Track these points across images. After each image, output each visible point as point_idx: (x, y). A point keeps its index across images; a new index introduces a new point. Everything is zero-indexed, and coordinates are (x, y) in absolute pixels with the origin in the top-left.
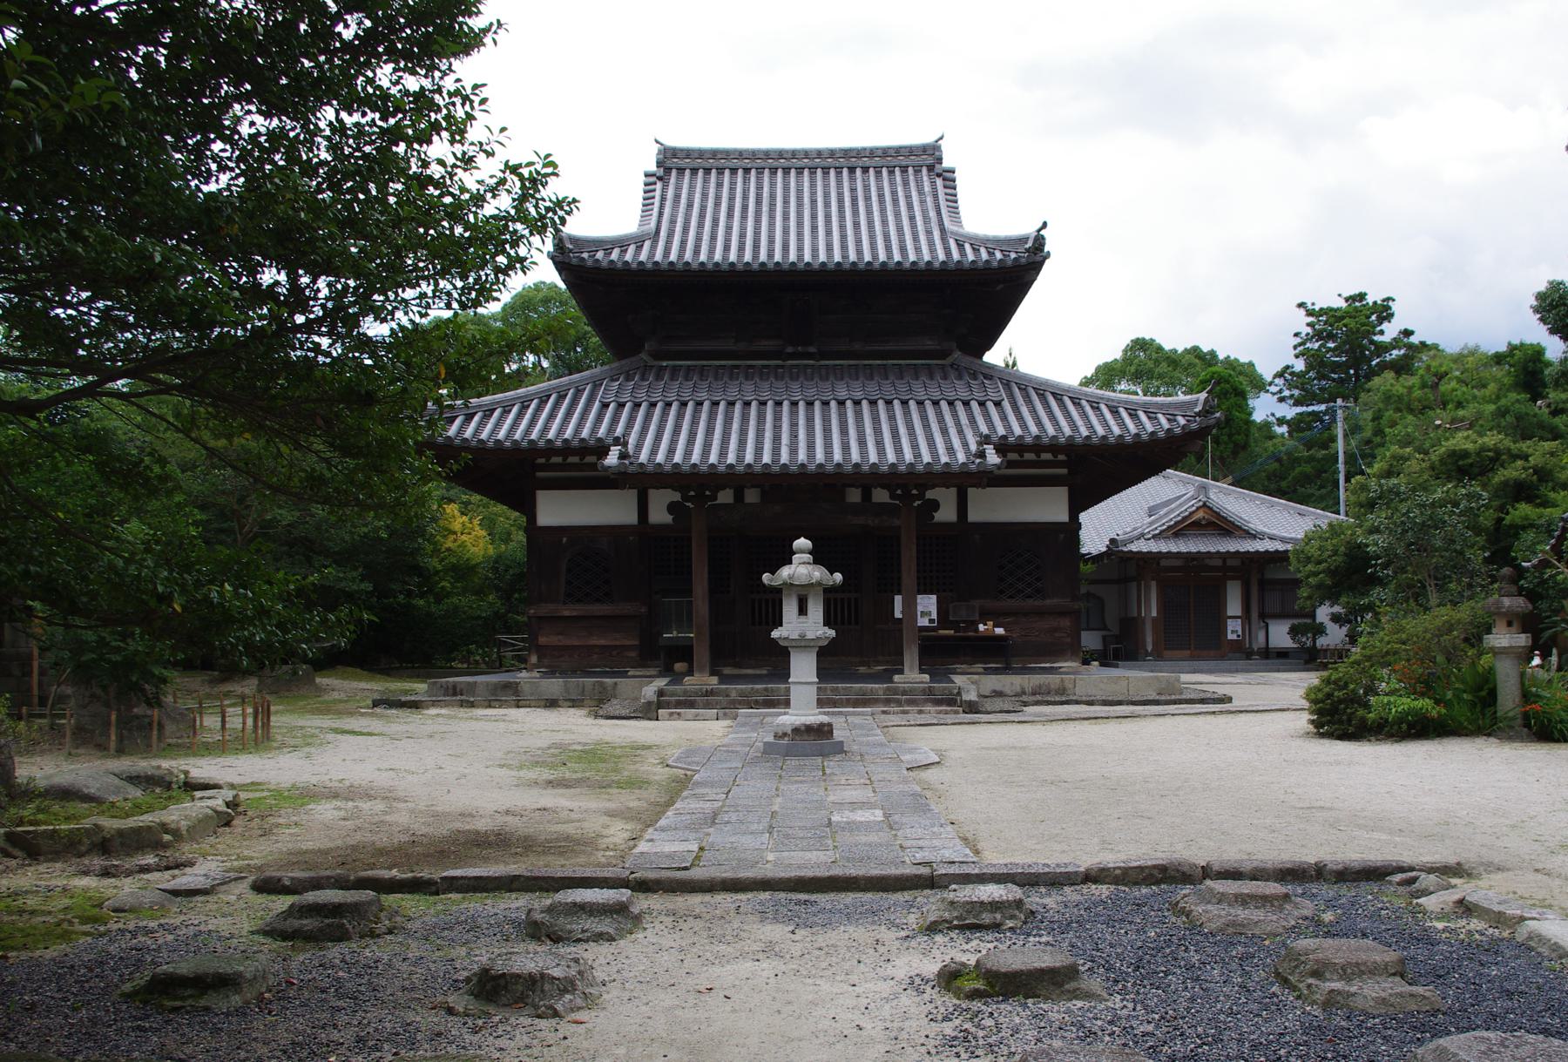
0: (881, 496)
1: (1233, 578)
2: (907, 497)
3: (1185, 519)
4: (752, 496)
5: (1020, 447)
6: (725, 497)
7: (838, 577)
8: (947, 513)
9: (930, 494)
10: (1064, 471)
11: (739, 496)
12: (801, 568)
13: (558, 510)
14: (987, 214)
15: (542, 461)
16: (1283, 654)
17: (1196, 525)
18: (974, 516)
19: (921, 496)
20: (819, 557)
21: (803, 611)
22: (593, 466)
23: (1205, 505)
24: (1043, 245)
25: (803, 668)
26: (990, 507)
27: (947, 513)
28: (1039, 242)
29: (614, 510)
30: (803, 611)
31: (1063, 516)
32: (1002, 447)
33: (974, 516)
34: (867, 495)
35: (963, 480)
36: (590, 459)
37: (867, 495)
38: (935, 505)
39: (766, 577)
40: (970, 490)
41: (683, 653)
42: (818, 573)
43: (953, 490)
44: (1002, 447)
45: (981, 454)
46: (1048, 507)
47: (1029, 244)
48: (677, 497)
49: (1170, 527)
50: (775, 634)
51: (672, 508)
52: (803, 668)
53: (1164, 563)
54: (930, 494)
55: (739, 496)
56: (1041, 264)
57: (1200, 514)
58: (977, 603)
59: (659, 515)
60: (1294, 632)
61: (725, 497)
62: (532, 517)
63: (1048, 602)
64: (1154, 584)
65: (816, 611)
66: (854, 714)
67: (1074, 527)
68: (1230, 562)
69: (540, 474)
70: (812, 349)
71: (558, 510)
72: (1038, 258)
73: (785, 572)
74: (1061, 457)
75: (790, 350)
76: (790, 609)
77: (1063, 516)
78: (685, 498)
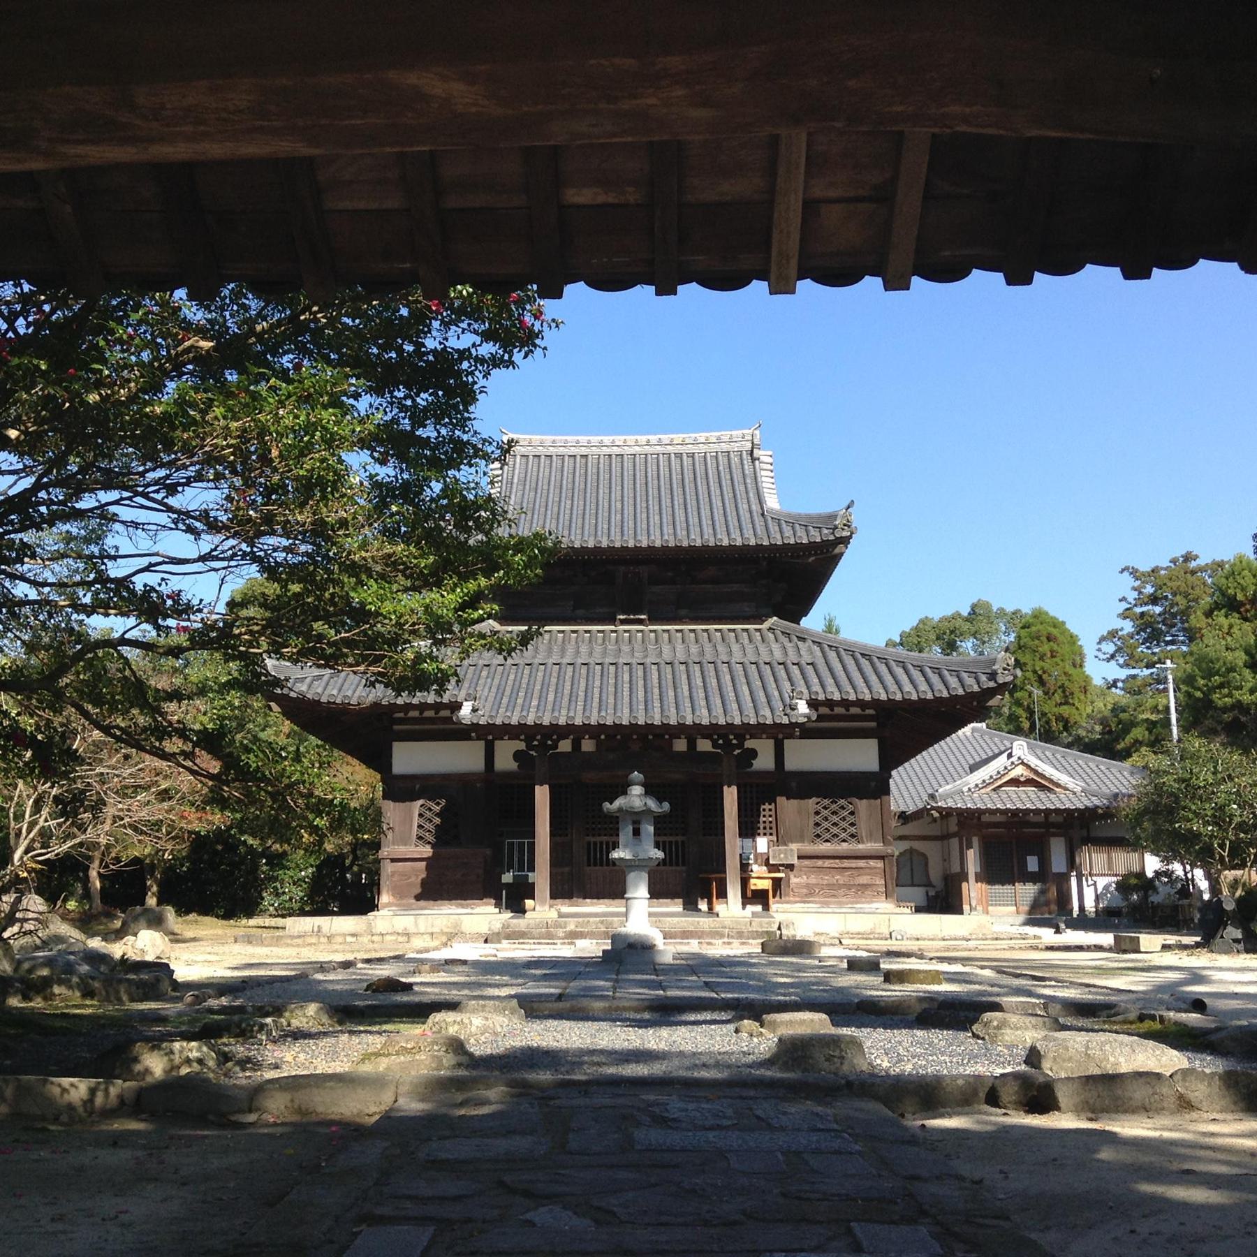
0: (704, 745)
1: (1054, 835)
4: (588, 745)
5: (830, 703)
6: (565, 746)
7: (666, 806)
10: (874, 724)
11: (576, 745)
12: (635, 797)
15: (402, 715)
18: (791, 764)
19: (741, 745)
20: (650, 790)
22: (448, 720)
27: (764, 761)
29: (462, 758)
33: (791, 764)
34: (692, 744)
35: (780, 733)
36: (445, 713)
37: (692, 744)
38: (753, 754)
39: (607, 805)
42: (652, 804)
43: (771, 742)
44: (812, 704)
48: (521, 746)
51: (517, 756)
53: (986, 818)
54: (750, 744)
55: (576, 745)
58: (794, 847)
61: (565, 746)
68: (1053, 818)
69: (396, 727)
73: (619, 802)
74: (870, 712)
76: (626, 833)
78: (530, 747)
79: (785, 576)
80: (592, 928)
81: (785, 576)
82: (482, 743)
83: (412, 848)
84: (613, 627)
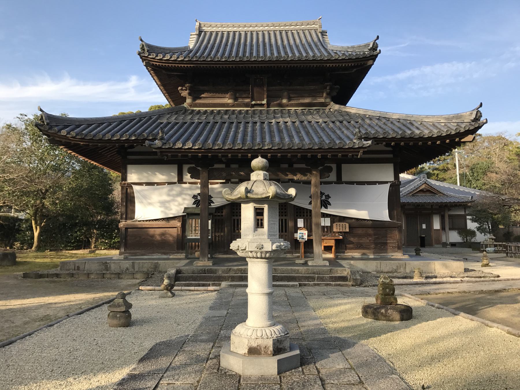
3: (417, 189)
10: (391, 156)
16: (453, 245)
17: (422, 191)
23: (425, 183)
24: (377, 47)
25: (257, 273)
28: (375, 47)
47: (371, 46)
49: (411, 192)
50: (234, 246)
52: (257, 273)
56: (376, 56)
57: (423, 186)
62: (124, 178)
66: (287, 286)
72: (375, 53)
75: (253, 103)
80: (232, 274)
82: (176, 166)
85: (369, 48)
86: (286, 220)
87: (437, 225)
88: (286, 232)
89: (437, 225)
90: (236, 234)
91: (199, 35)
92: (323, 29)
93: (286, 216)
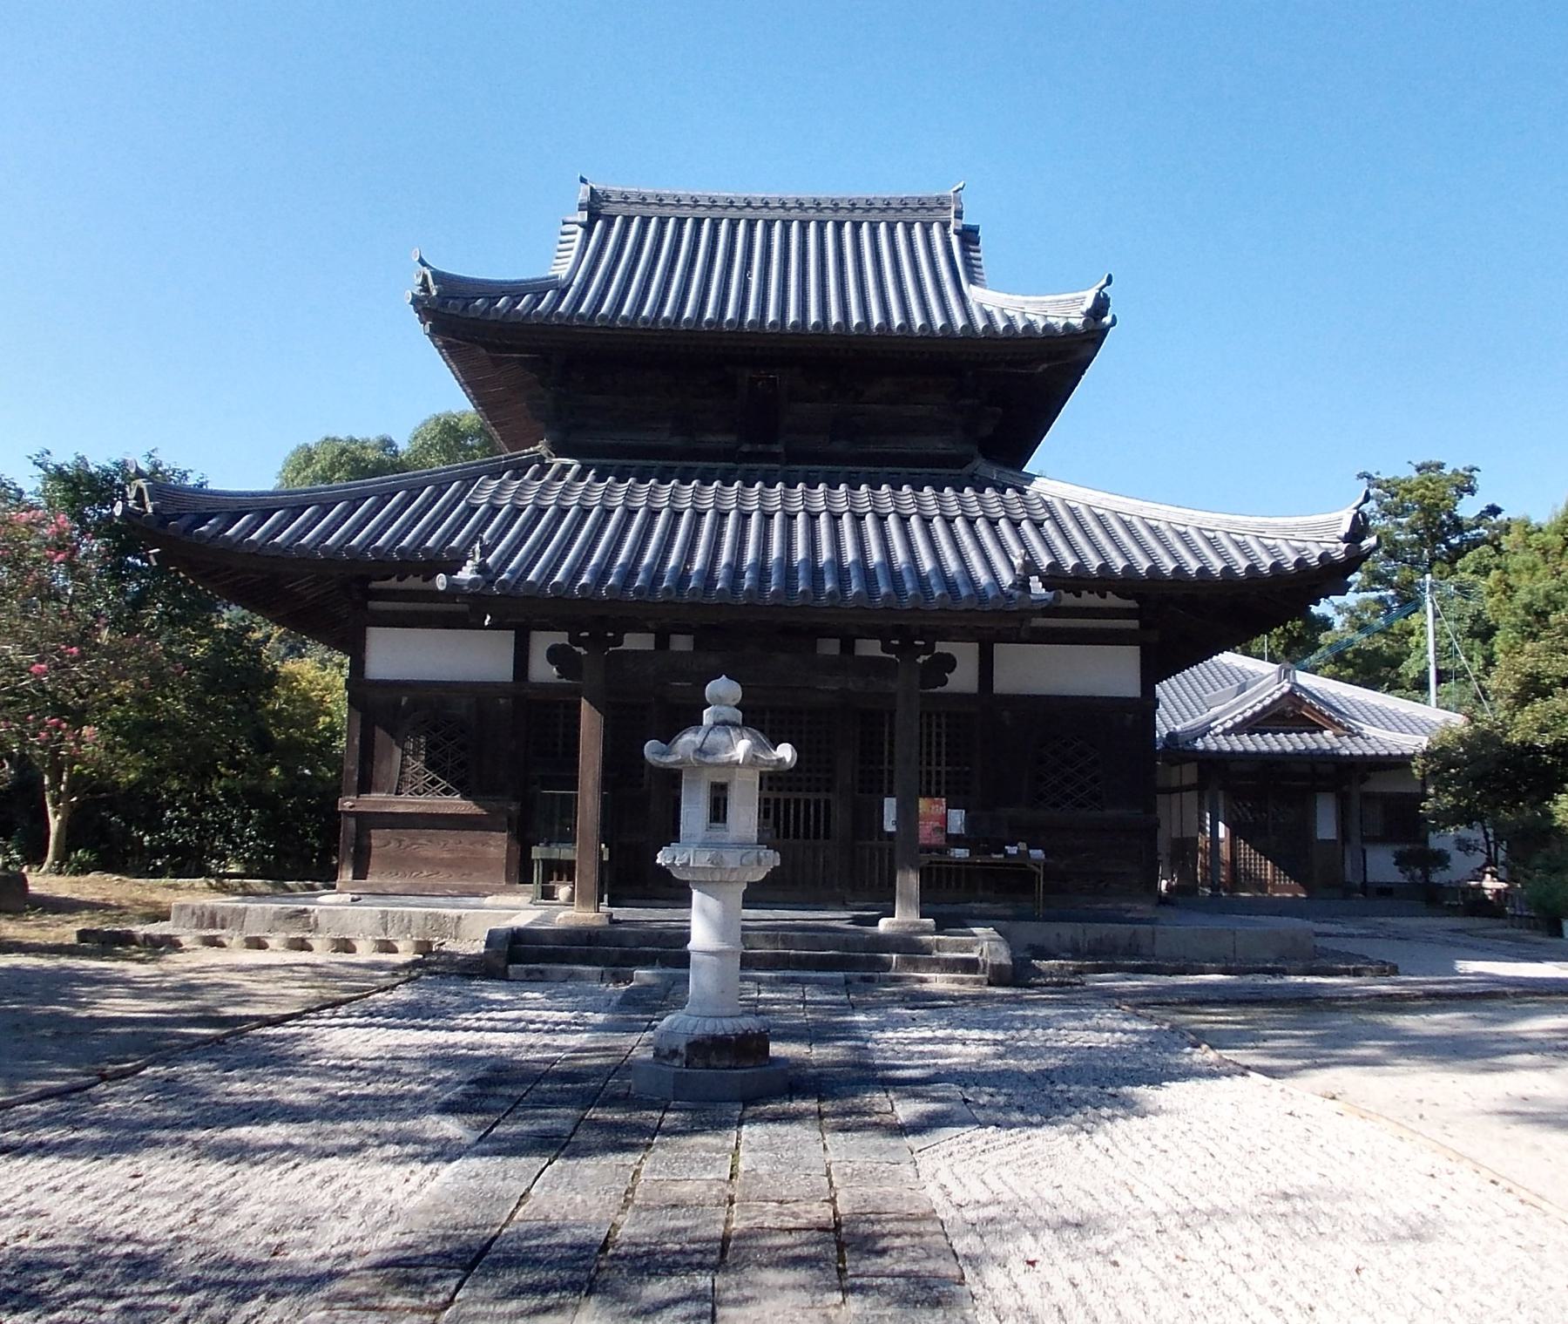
0: (870, 648)
1: (1325, 790)
2: (907, 650)
6: (637, 642)
7: (786, 752)
8: (963, 679)
9: (941, 647)
10: (1134, 624)
13: (399, 655)
14: (1014, 299)
16: (1385, 891)
18: (1004, 682)
19: (929, 649)
21: (718, 812)
26: (1030, 670)
27: (963, 679)
29: (478, 657)
30: (718, 812)
31: (1132, 689)
32: (1054, 577)
33: (1004, 682)
34: (848, 647)
38: (949, 663)
39: (651, 748)
40: (1000, 650)
41: (564, 870)
43: (974, 647)
45: (1023, 584)
46: (1107, 672)
48: (562, 638)
51: (554, 655)
54: (941, 647)
55: (662, 642)
56: (1104, 332)
59: (543, 671)
60: (1402, 861)
63: (1110, 813)
64: (1221, 793)
65: (744, 816)
67: (1147, 704)
70: (778, 448)
71: (399, 655)
75: (746, 448)
76: (693, 811)
77: (1132, 689)
78: (575, 640)
79: (997, 396)
81: (997, 396)
83: (393, 798)
84: (731, 465)
85: (1084, 309)
86: (827, 802)
87: (1326, 828)
88: (827, 837)
89: (1326, 828)
90: (672, 834)
91: (588, 228)
92: (967, 220)
93: (828, 790)
